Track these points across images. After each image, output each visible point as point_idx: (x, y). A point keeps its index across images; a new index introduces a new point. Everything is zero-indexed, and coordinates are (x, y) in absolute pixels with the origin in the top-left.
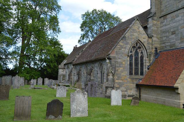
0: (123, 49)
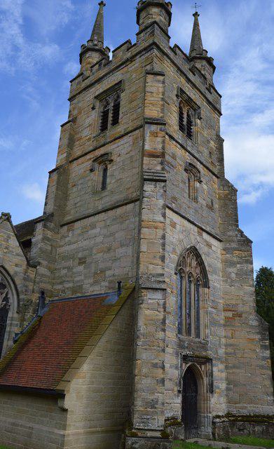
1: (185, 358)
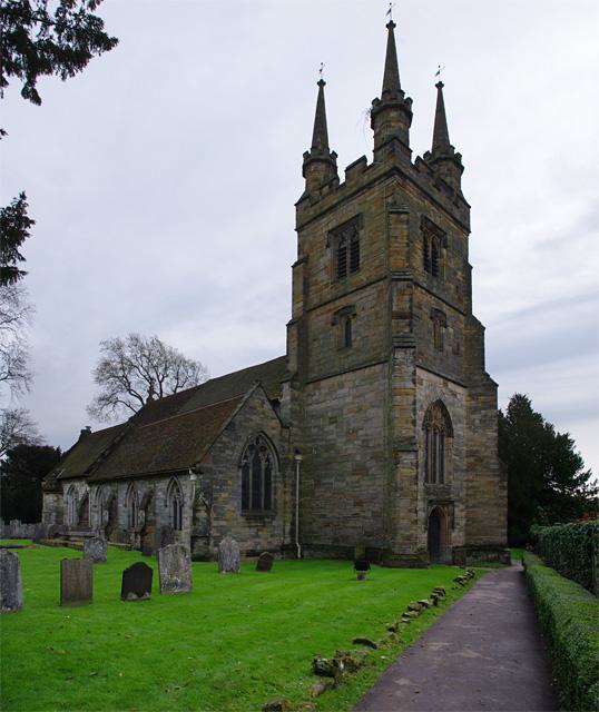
0: (228, 452)
1: (430, 502)
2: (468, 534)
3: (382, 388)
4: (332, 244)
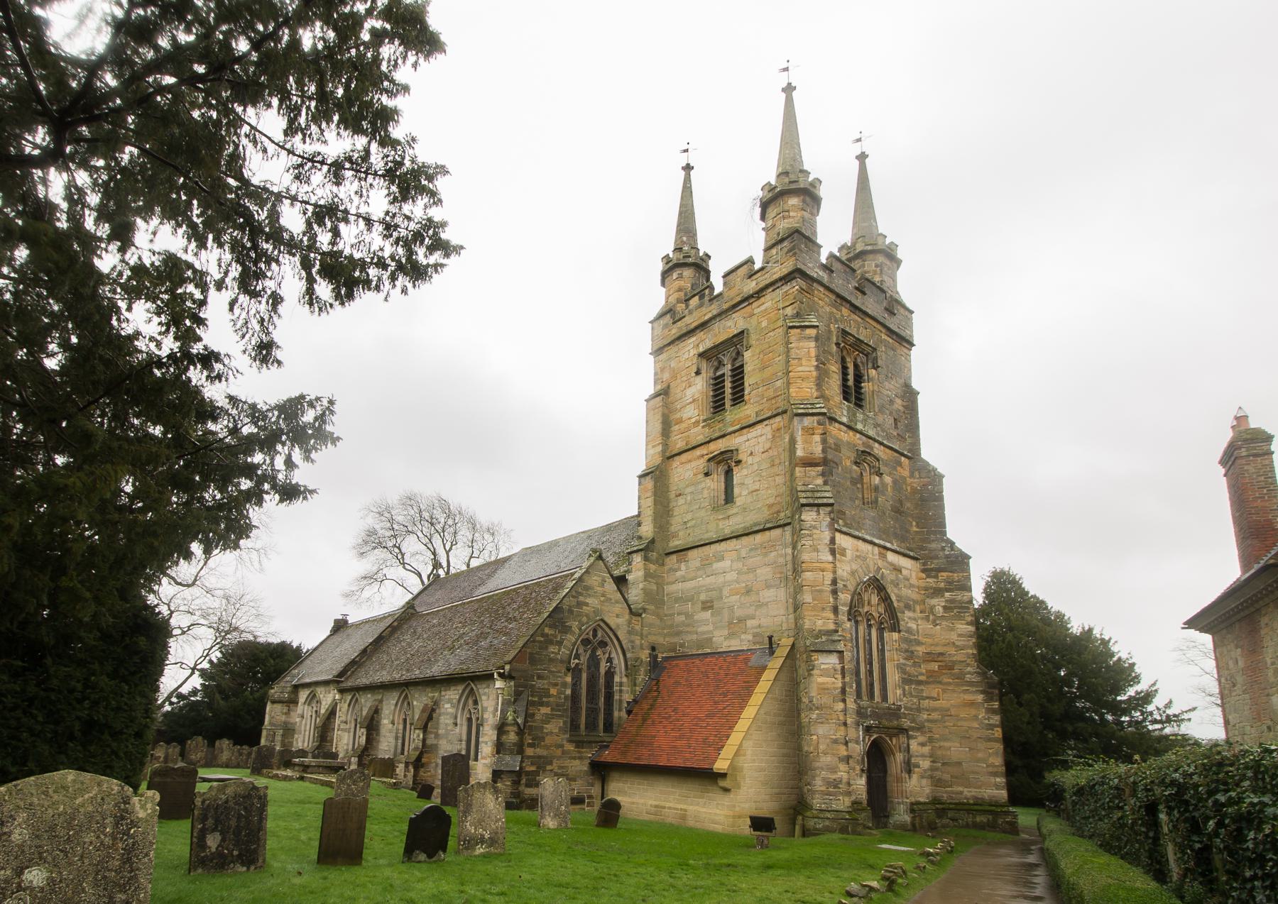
0: (552, 649)
1: (868, 730)
2: (937, 783)
3: (781, 560)
4: (703, 371)
